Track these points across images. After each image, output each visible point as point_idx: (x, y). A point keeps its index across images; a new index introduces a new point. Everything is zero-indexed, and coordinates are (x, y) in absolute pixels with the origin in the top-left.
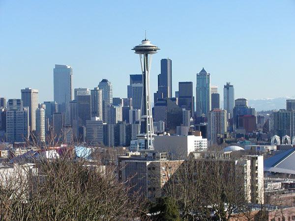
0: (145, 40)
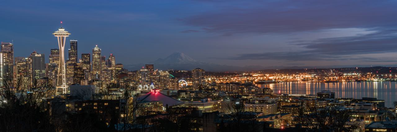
0: (61, 28)
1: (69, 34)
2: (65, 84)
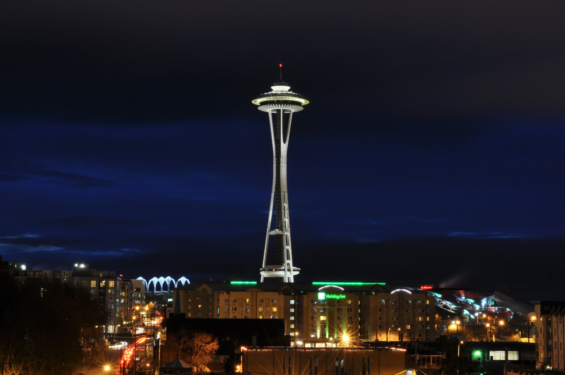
1: (303, 101)
2: (290, 262)
